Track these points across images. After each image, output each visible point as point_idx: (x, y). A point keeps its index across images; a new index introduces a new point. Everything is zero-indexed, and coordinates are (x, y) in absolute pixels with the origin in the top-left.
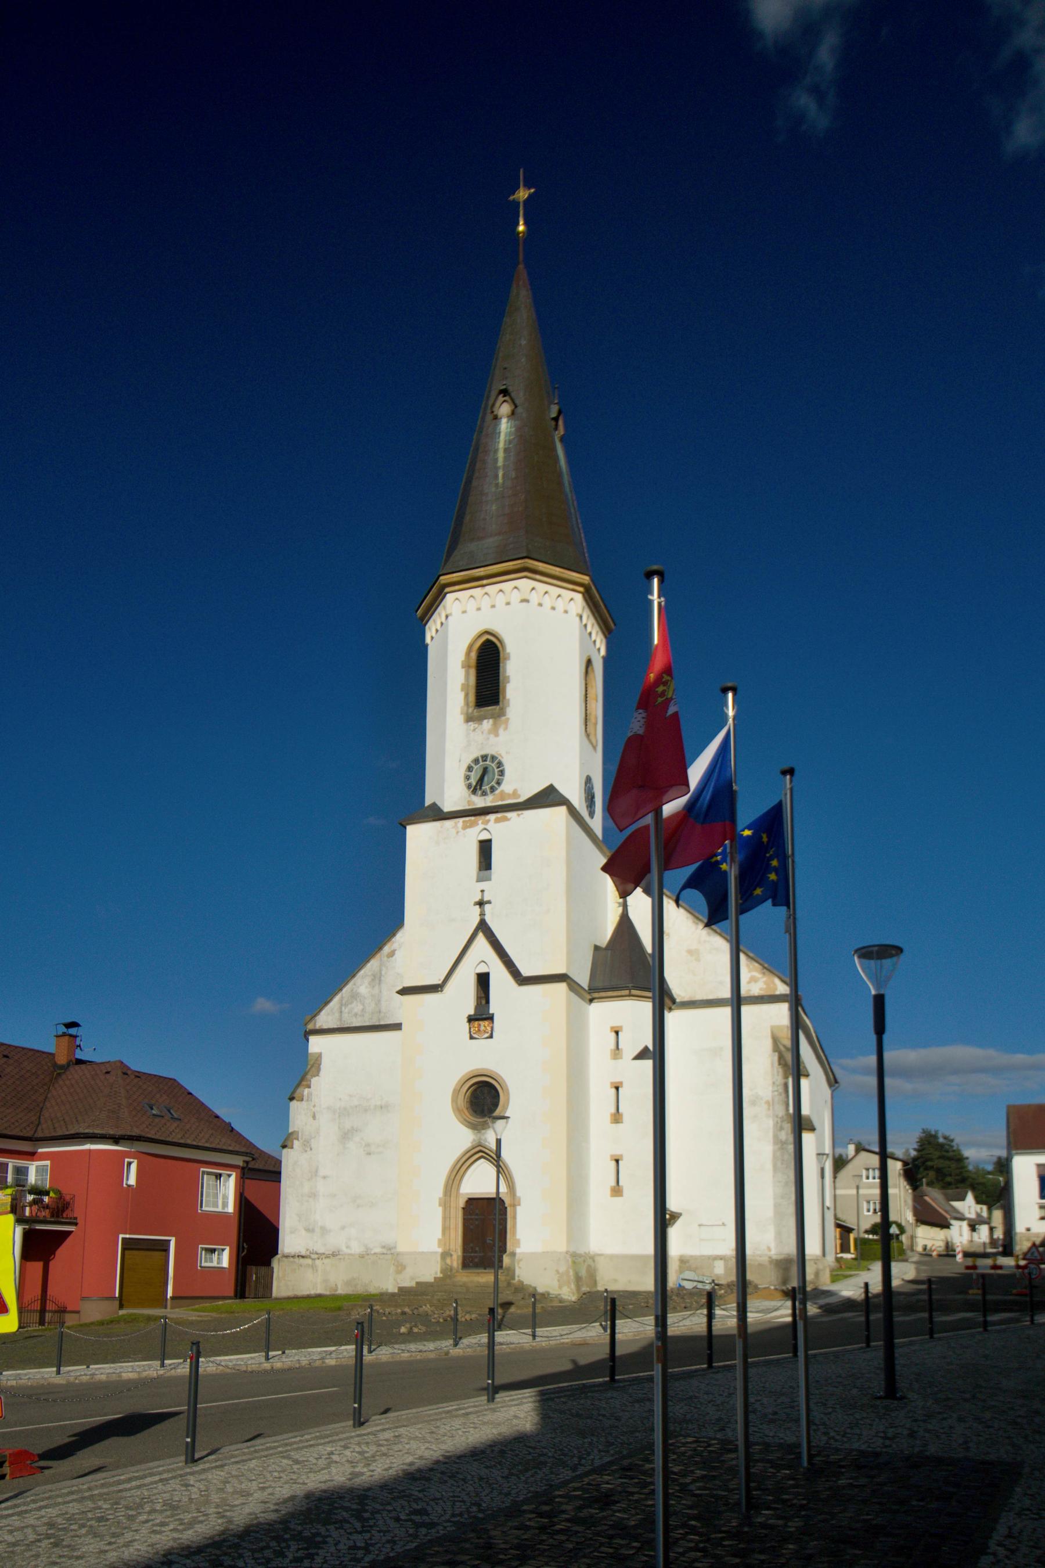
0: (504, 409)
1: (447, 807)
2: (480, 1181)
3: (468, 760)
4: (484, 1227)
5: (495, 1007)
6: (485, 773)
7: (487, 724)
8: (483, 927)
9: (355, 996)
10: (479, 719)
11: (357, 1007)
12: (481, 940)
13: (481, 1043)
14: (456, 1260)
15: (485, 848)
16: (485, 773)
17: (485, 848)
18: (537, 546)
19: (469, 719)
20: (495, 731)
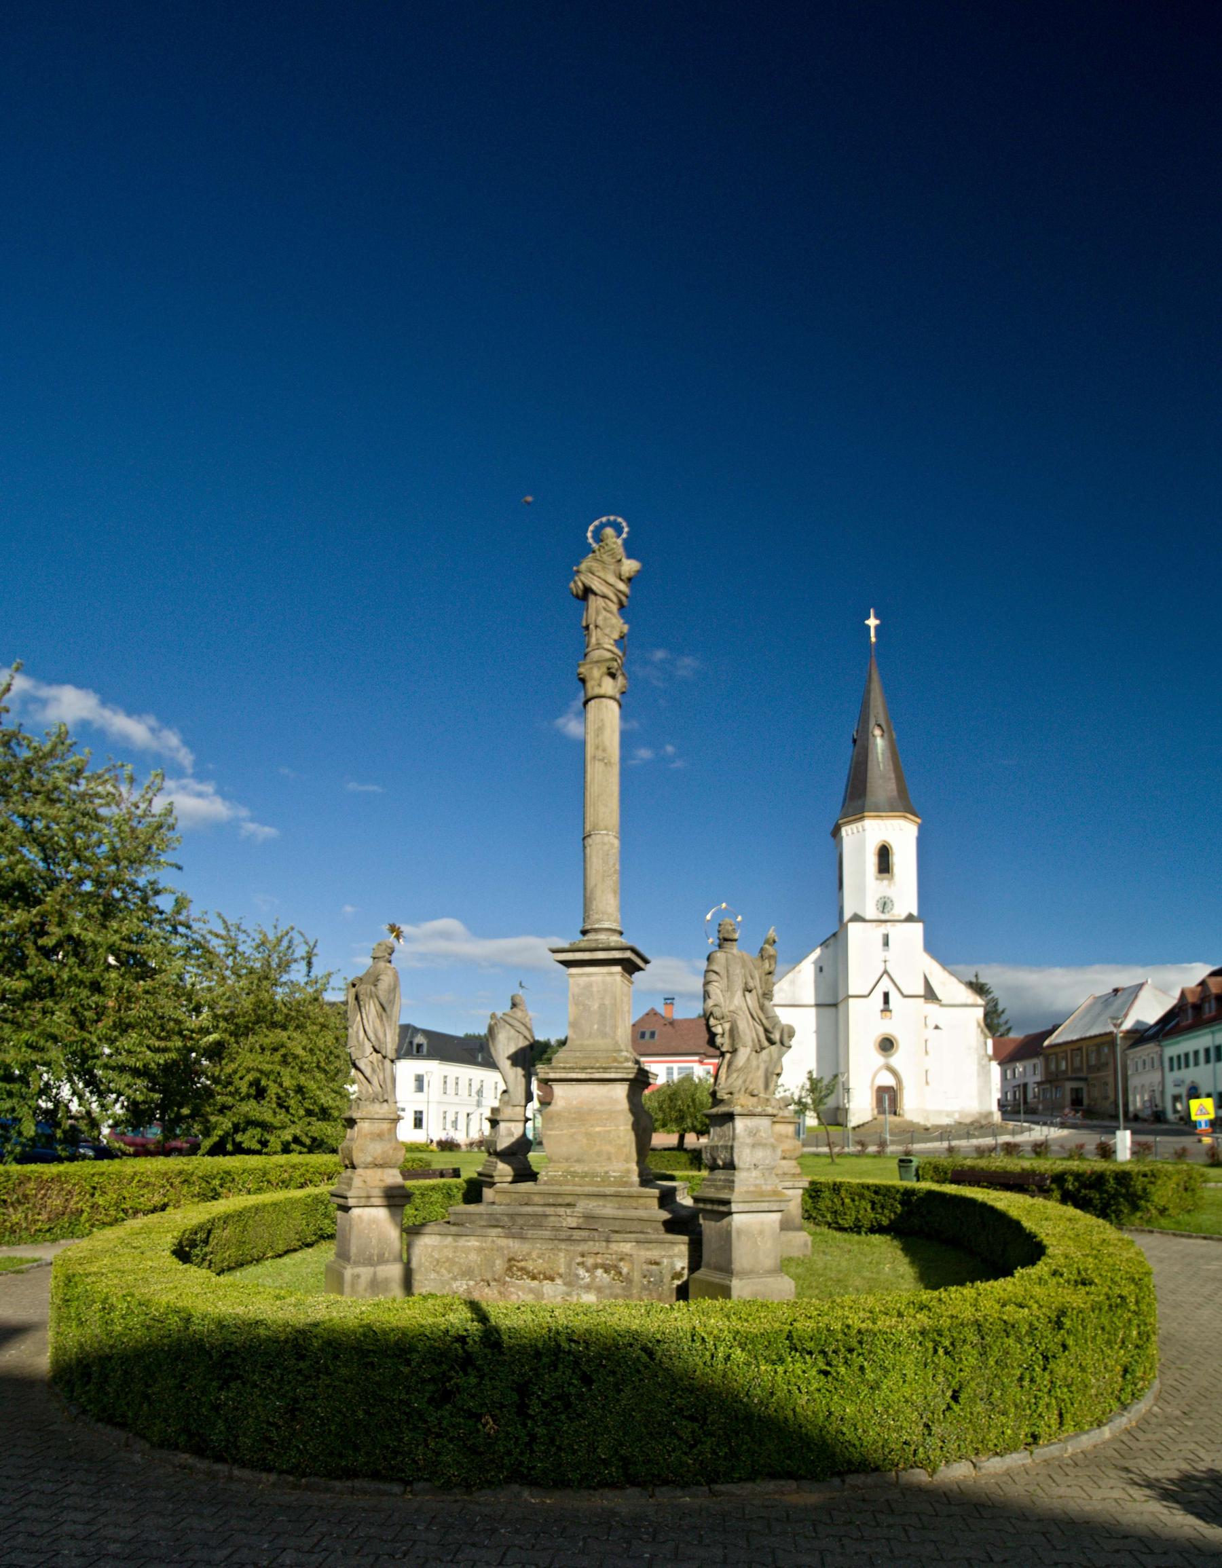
0: (877, 732)
1: (867, 918)
2: (887, 1080)
3: (877, 897)
4: (888, 1098)
5: (892, 1005)
6: (884, 905)
7: (885, 882)
8: (886, 972)
10: (882, 879)
12: (885, 976)
13: (887, 1021)
14: (876, 1112)
16: (884, 905)
18: (904, 805)
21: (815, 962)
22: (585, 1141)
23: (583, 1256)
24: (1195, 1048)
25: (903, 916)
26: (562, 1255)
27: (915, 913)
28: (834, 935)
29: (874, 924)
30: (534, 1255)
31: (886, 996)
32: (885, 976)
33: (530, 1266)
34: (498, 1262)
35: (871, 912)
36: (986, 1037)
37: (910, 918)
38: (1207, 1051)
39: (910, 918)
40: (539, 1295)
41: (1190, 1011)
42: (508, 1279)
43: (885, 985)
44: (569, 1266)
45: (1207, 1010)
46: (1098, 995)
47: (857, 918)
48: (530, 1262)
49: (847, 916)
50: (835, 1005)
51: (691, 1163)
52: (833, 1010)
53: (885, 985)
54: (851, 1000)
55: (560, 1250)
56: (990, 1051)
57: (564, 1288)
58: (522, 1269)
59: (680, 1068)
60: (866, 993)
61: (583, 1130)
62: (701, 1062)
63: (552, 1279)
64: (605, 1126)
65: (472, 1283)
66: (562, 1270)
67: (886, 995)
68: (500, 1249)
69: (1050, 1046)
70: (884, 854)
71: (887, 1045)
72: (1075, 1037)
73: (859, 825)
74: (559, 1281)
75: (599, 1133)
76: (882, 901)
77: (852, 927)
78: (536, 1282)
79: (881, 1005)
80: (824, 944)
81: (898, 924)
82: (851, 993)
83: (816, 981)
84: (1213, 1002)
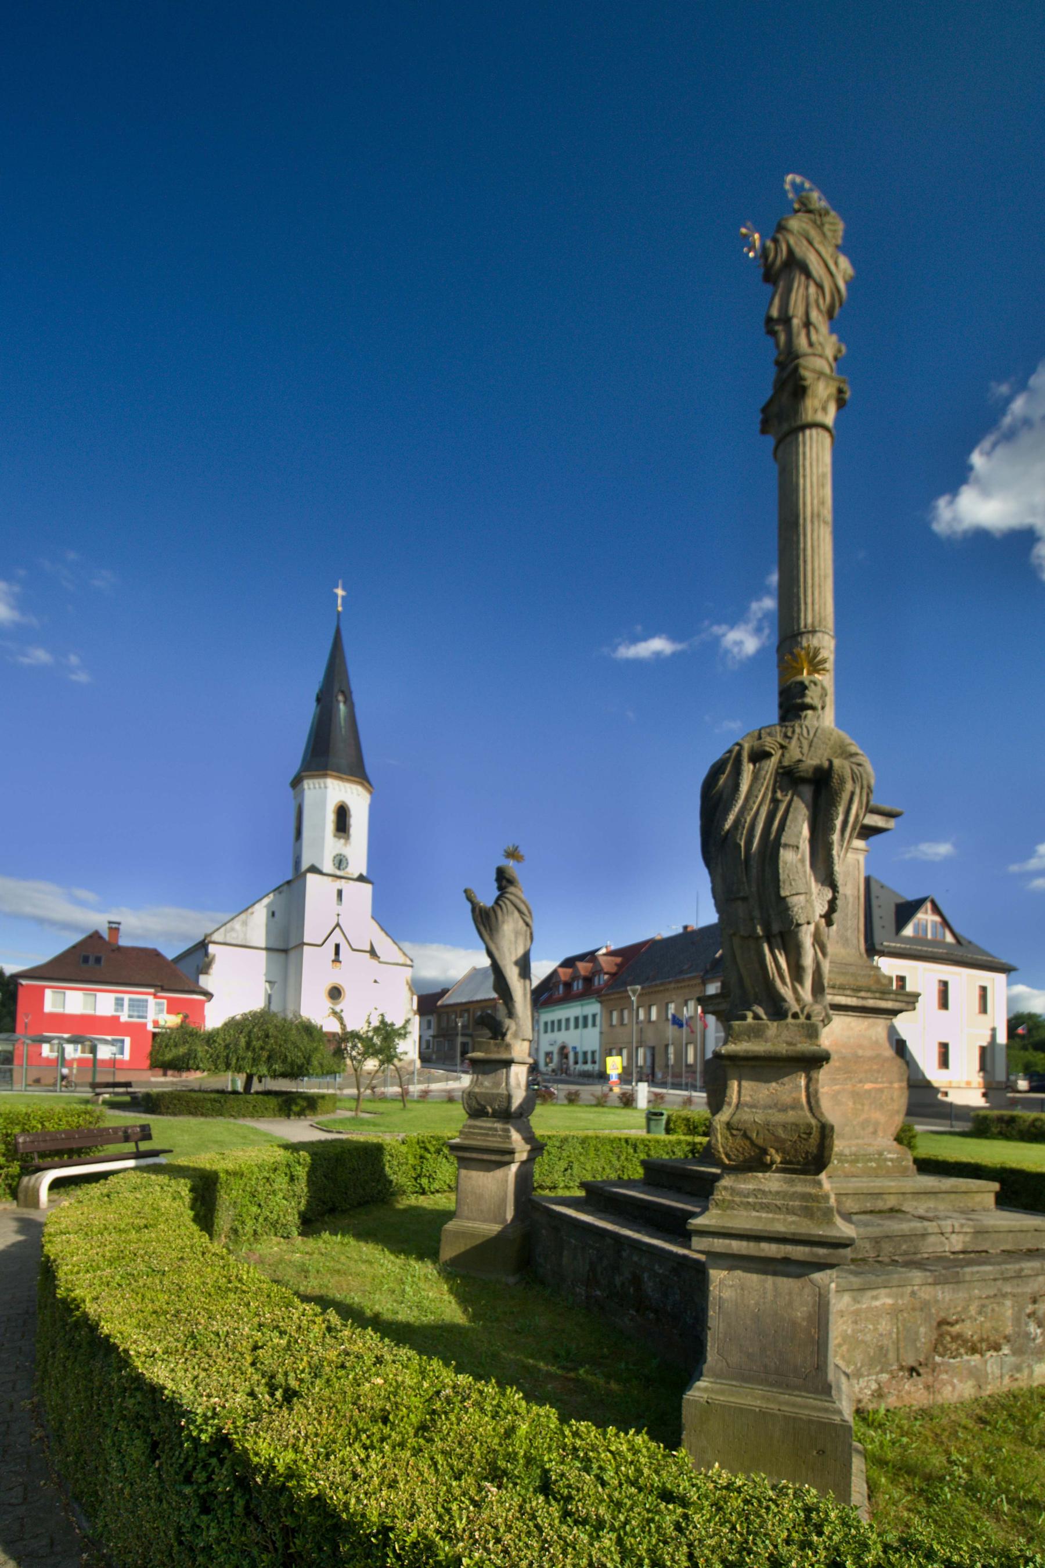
1: (325, 871)
5: (341, 958)
6: (340, 861)
7: (342, 841)
8: (338, 925)
9: (233, 929)
10: (340, 838)
11: (234, 935)
15: (340, 893)
16: (340, 861)
17: (340, 893)
19: (335, 836)
20: (345, 845)
21: (268, 906)
22: (850, 1104)
23: (1035, 1301)
24: (567, 1016)
25: (356, 876)
26: (1008, 1303)
27: (365, 873)
28: (288, 883)
29: (330, 878)
30: (973, 1310)
31: (337, 947)
32: (337, 929)
33: (967, 1329)
34: (922, 1330)
35: (328, 867)
36: (413, 994)
37: (361, 878)
38: (577, 1019)
39: (361, 878)
40: (978, 1376)
41: (561, 987)
42: (938, 1359)
43: (337, 937)
44: (1017, 1320)
45: (575, 988)
46: (478, 967)
47: (314, 869)
48: (968, 1323)
49: (305, 866)
50: (285, 951)
51: (280, 1110)
52: (282, 955)
53: (337, 937)
54: (305, 948)
55: (1004, 1296)
56: (415, 1007)
57: (1012, 1359)
58: (955, 1338)
59: (130, 1000)
60: (320, 943)
61: (849, 1087)
62: (155, 996)
63: (997, 1348)
64: (876, 1082)
65: (885, 1377)
66: (1009, 1330)
67: (337, 947)
68: (925, 1306)
69: (442, 1006)
70: (342, 814)
71: (335, 993)
72: (464, 1000)
73: (321, 781)
74: (1006, 1350)
75: (869, 1092)
76: (338, 858)
77: (311, 877)
78: (977, 1356)
79: (333, 957)
80: (277, 890)
81: (351, 882)
82: (306, 940)
83: (267, 925)
84: (581, 982)
